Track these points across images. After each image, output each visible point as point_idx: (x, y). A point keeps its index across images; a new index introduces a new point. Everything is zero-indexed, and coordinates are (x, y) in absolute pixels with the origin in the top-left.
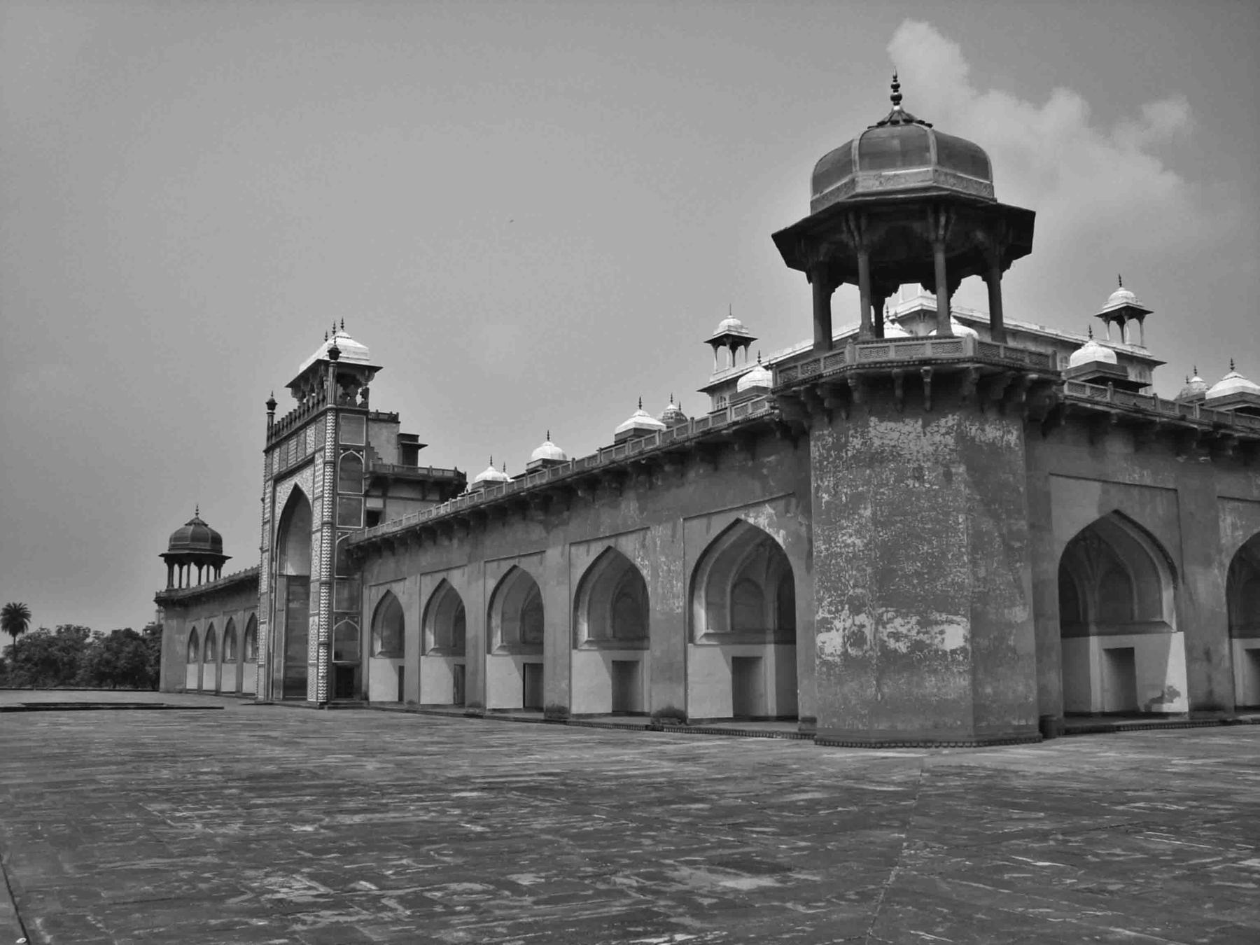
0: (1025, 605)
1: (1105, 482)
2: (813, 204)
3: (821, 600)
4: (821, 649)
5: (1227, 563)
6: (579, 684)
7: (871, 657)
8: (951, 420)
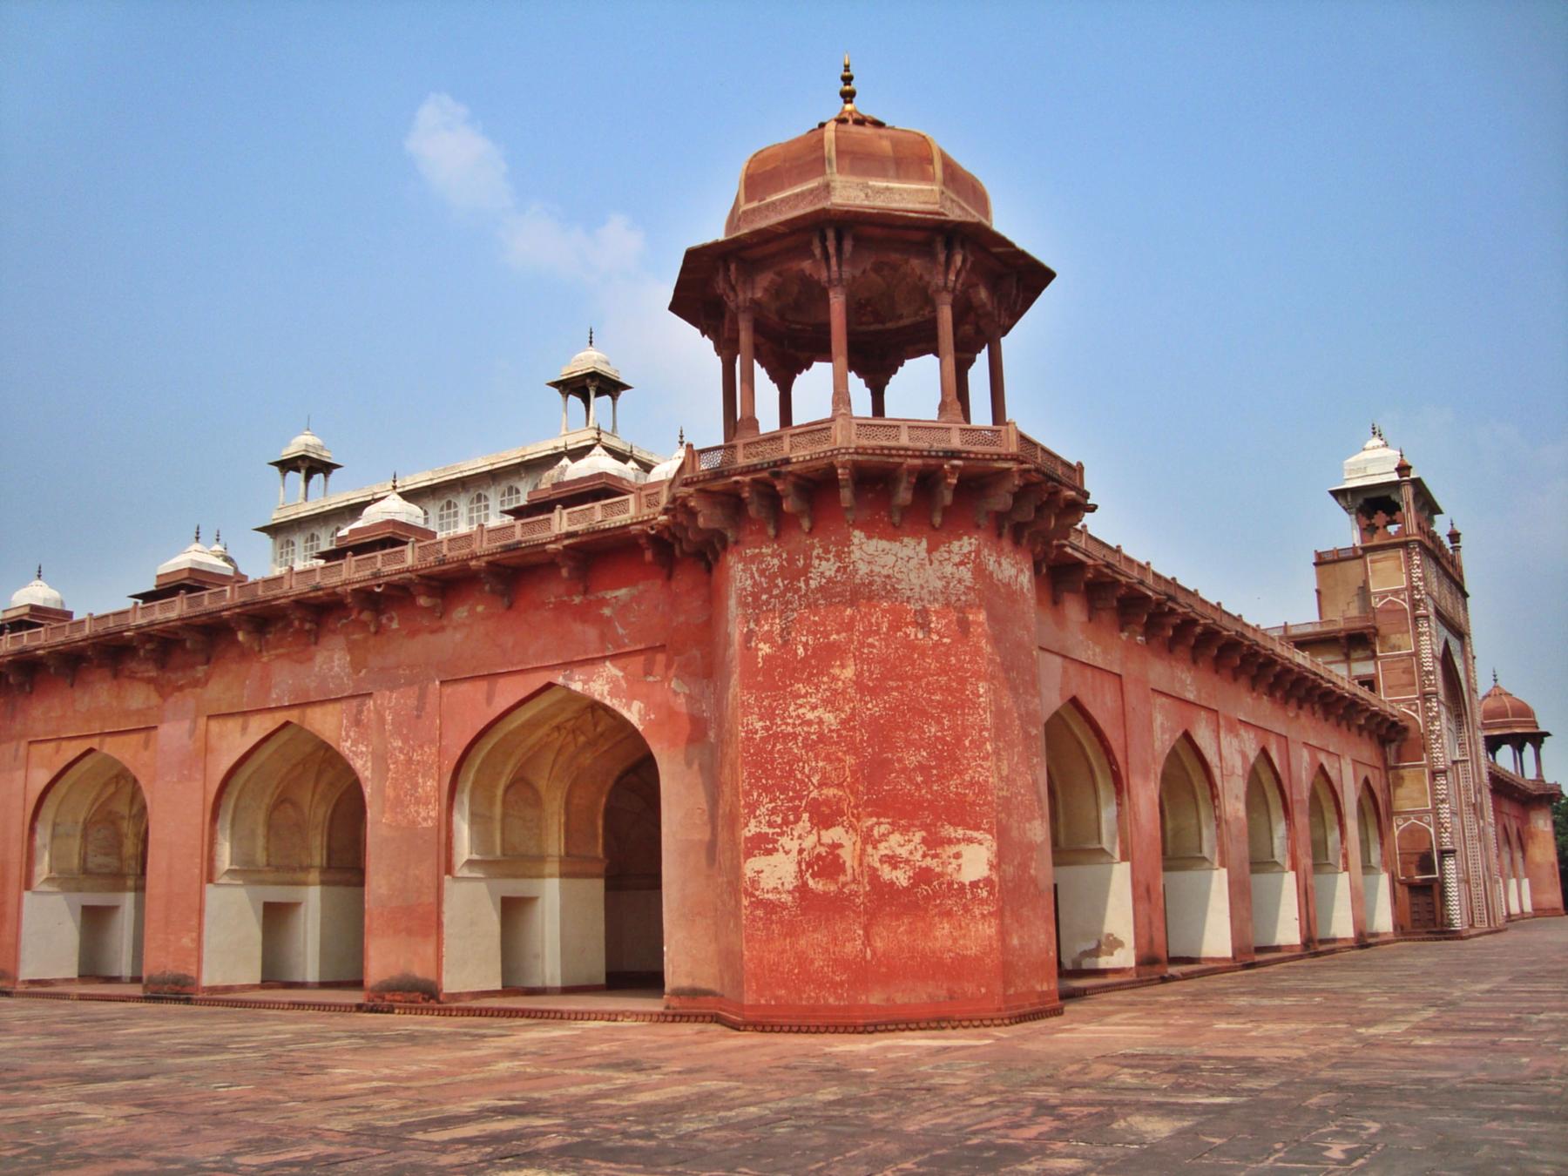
0: (1042, 817)
1: (1065, 657)
2: (734, 220)
3: (752, 808)
4: (754, 882)
5: (1159, 770)
6: (213, 937)
7: (856, 894)
8: (965, 545)
